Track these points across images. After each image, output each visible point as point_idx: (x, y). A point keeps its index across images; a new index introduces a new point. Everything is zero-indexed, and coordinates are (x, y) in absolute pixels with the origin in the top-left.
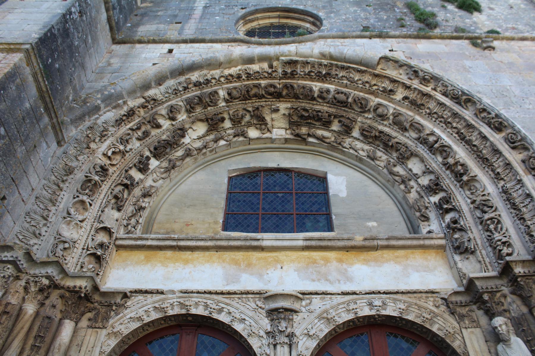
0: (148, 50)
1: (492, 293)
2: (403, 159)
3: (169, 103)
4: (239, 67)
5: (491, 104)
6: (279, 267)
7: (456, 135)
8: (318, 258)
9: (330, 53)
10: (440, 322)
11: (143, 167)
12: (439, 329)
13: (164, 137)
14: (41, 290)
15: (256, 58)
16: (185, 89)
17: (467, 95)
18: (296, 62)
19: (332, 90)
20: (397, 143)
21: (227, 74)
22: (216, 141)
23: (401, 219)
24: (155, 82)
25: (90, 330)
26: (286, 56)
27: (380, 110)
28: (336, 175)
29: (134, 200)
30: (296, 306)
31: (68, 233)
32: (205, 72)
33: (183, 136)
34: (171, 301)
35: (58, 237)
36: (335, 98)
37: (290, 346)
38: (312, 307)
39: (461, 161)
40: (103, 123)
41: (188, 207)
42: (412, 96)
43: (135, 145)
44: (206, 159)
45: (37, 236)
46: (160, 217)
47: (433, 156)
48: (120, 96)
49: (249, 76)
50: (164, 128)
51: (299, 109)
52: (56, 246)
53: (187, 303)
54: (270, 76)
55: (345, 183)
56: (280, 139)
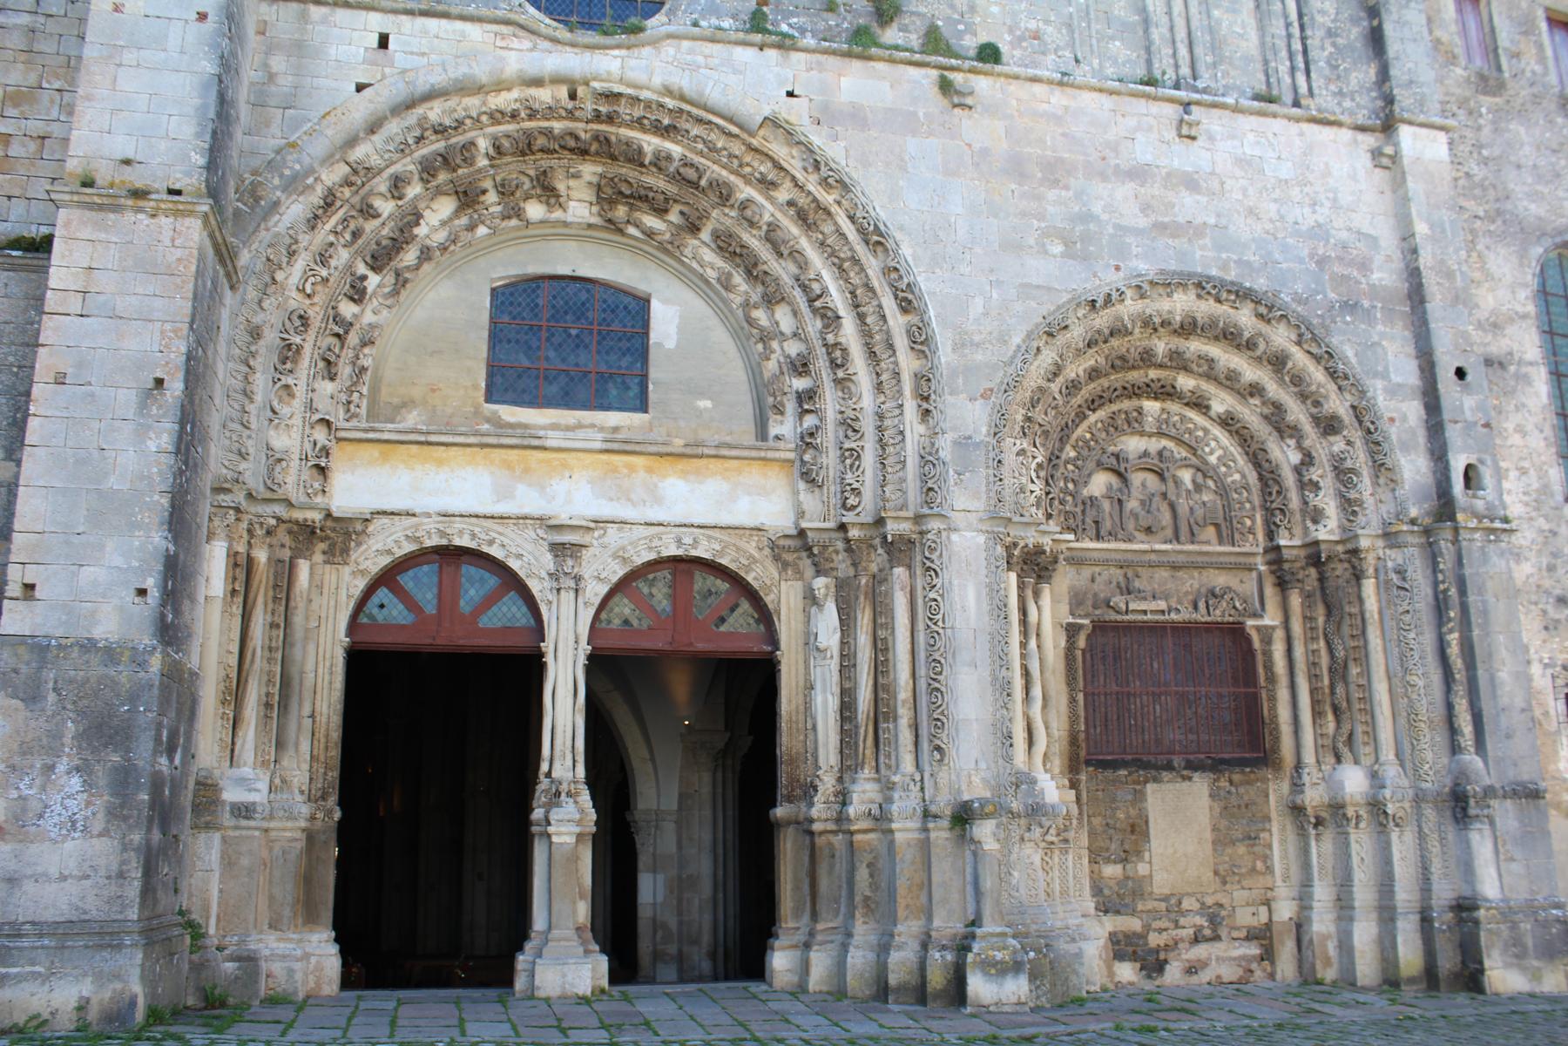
0: (336, 30)
1: (825, 547)
2: (771, 300)
3: (391, 170)
5: (909, 259)
6: (567, 475)
7: (849, 296)
9: (681, 89)
11: (357, 294)
12: (755, 579)
13: (385, 232)
14: (269, 533)
15: (547, 80)
16: (419, 139)
17: (881, 235)
18: (618, 96)
20: (765, 273)
21: (494, 107)
22: (471, 228)
26: (602, 81)
27: (748, 213)
28: (666, 301)
29: (351, 354)
31: (280, 441)
33: (418, 224)
36: (680, 174)
37: (577, 591)
38: (605, 540)
39: (843, 340)
40: (288, 228)
42: (803, 201)
43: (342, 256)
45: (243, 455)
46: (389, 374)
47: (811, 315)
48: (310, 171)
49: (533, 114)
50: (385, 215)
52: (271, 470)
53: (449, 531)
54: (571, 115)
55: (676, 321)
56: (579, 224)
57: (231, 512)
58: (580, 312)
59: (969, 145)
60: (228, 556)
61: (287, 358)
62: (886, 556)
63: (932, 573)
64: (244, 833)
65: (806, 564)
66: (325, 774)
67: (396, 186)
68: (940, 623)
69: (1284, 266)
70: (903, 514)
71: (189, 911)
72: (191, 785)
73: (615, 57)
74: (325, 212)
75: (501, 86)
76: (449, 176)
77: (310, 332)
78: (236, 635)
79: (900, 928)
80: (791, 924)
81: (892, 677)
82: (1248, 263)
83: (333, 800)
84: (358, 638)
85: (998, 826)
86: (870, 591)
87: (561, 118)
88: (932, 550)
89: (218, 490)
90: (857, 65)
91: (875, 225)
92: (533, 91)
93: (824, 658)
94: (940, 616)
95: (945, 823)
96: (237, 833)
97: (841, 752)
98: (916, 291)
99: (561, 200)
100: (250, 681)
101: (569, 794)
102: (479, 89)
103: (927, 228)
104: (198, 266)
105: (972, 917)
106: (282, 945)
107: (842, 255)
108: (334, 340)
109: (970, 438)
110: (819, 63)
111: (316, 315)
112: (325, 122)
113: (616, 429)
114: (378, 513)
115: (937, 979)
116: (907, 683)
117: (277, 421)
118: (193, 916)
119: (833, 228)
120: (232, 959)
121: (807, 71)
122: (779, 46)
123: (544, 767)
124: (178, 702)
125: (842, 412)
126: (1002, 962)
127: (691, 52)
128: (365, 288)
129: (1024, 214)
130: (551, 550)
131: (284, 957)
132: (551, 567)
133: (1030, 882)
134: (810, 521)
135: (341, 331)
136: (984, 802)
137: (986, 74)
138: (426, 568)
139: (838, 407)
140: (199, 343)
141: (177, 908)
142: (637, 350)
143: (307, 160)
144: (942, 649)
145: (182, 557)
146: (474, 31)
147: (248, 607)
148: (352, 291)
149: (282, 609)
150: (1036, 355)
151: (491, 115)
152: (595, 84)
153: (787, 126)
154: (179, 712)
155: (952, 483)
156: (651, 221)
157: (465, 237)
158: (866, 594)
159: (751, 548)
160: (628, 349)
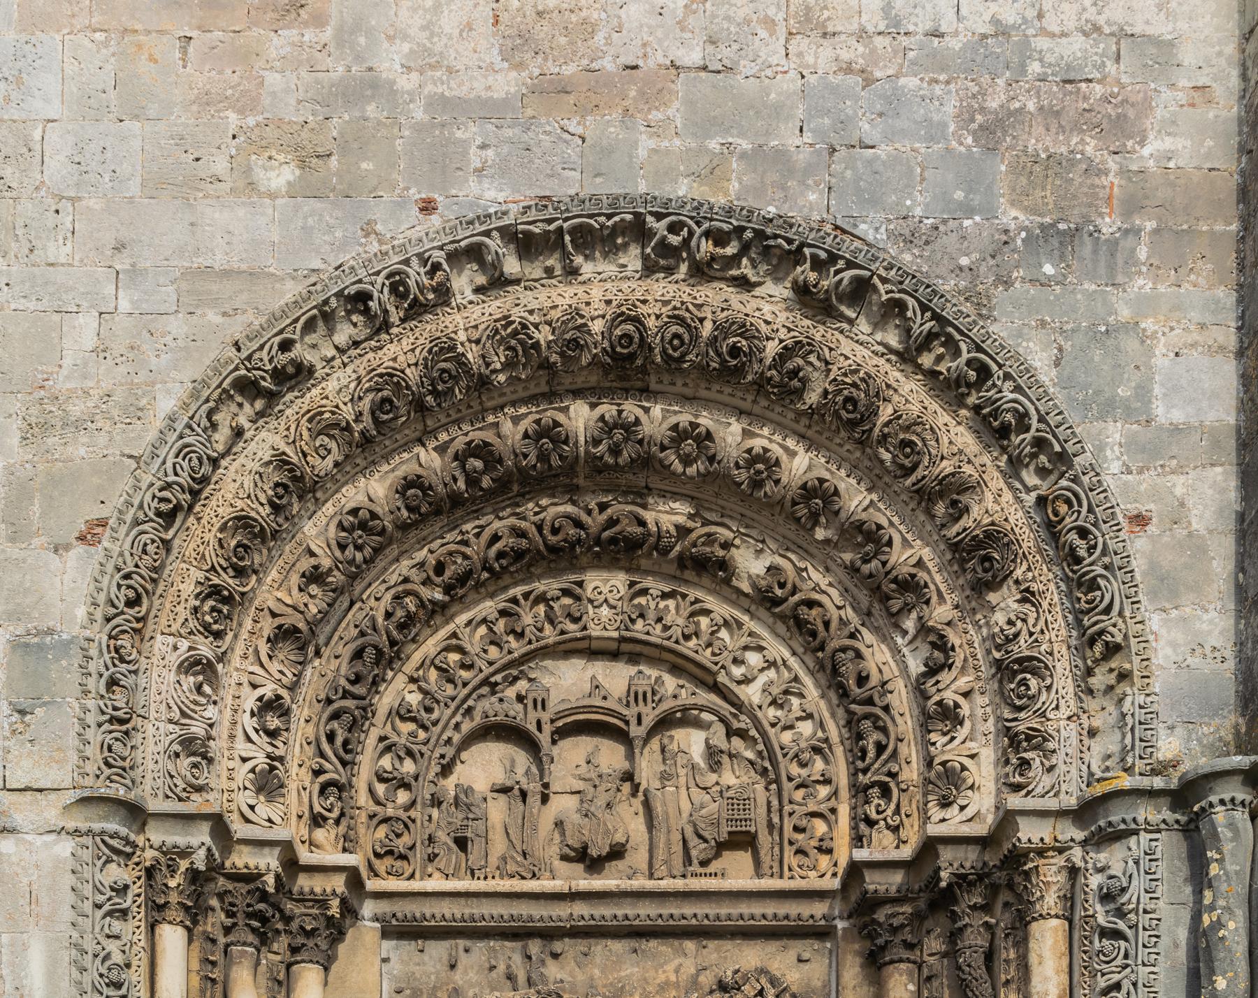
69: (883, 151)
82: (780, 155)
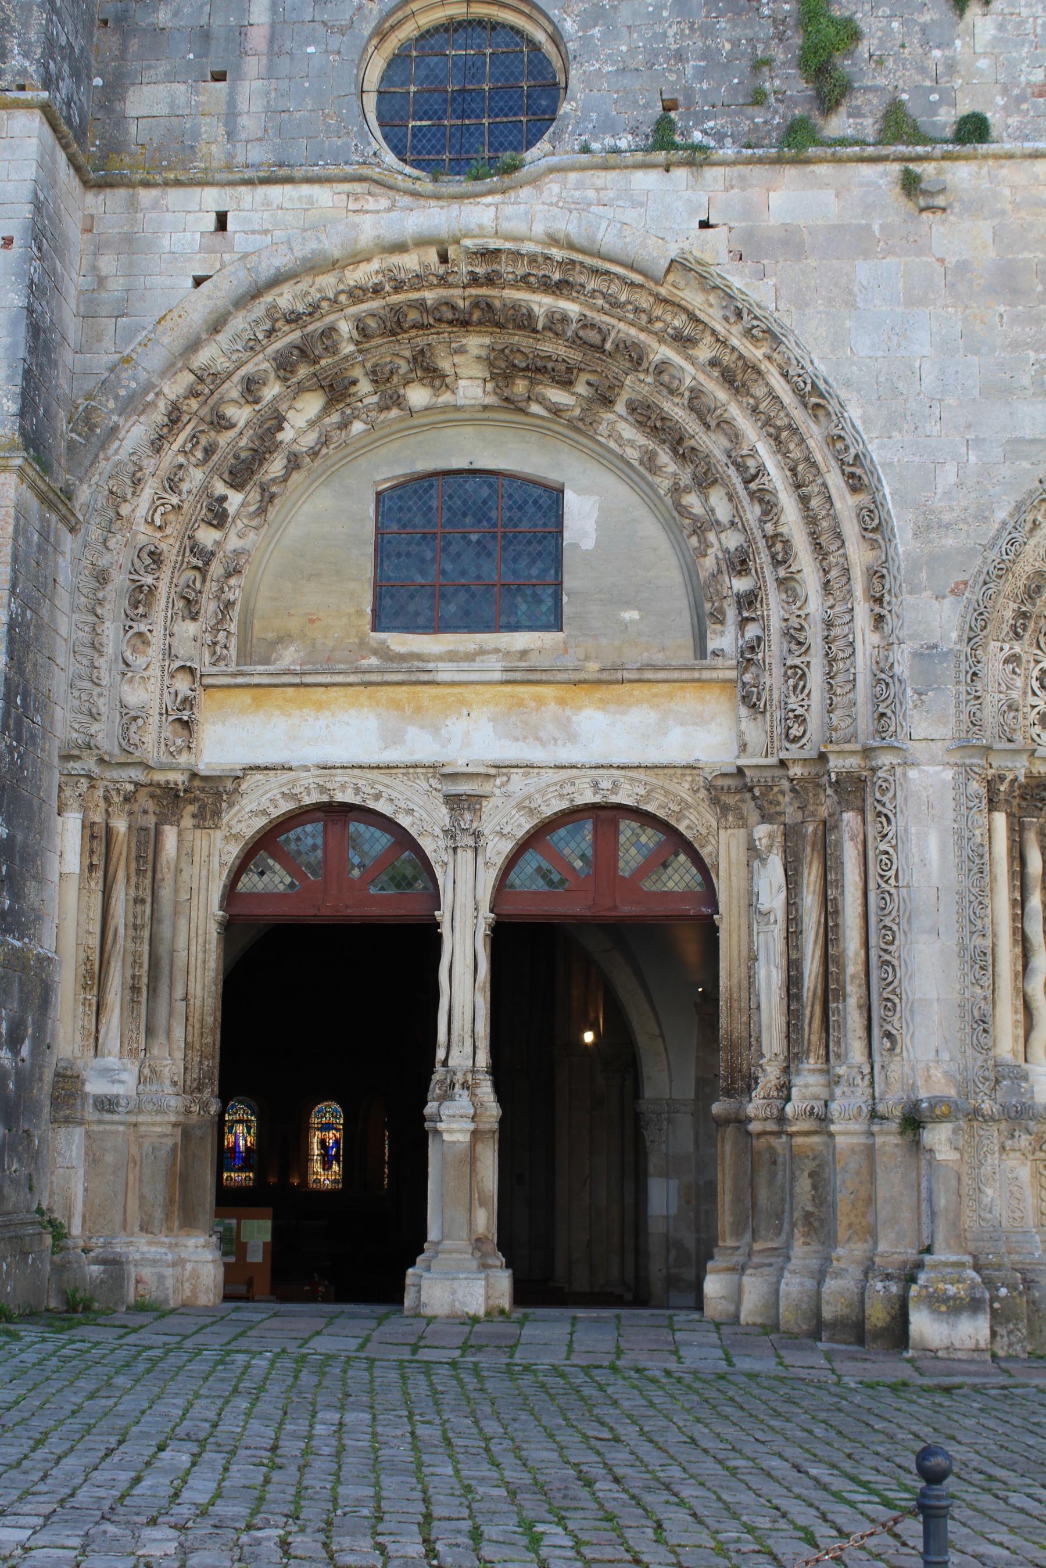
2: (705, 481)
4: (375, 265)
5: (858, 423)
7: (789, 474)
8: (526, 696)
9: (567, 236)
10: (692, 818)
11: (218, 518)
12: (688, 827)
13: (243, 443)
14: (127, 800)
16: (270, 333)
17: (821, 396)
19: (572, 315)
20: (693, 449)
21: (352, 283)
22: (344, 425)
23: (686, 602)
24: (207, 331)
25: (198, 832)
26: (474, 237)
27: (665, 378)
28: (580, 492)
30: (486, 788)
31: (135, 696)
32: (303, 286)
33: (280, 429)
34: (305, 782)
35: (125, 711)
37: (476, 849)
38: (510, 788)
39: (783, 530)
41: (309, 580)
42: (727, 359)
43: (196, 477)
44: (329, 462)
45: (94, 716)
46: (263, 605)
48: (149, 386)
50: (241, 424)
51: (507, 351)
52: (126, 730)
53: (329, 786)
54: (443, 281)
55: (595, 514)
56: (473, 406)
57: (83, 780)
58: (481, 512)
59: (942, 261)
60: (83, 827)
61: (139, 602)
62: (835, 798)
63: (883, 819)
64: (108, 1127)
65: (749, 808)
66: (201, 1063)
67: (249, 390)
68: (892, 881)
70: (847, 747)
71: (50, 1210)
72: (48, 1076)
73: (488, 205)
74: (170, 430)
75: (358, 258)
76: (312, 370)
77: (164, 568)
78: (97, 914)
79: (840, 1251)
80: (730, 1243)
81: (841, 946)
83: (207, 1093)
84: (236, 911)
85: (955, 1131)
86: (819, 840)
87: (432, 286)
88: (884, 791)
89: (67, 758)
90: (791, 172)
91: (813, 384)
92: (396, 259)
93: (768, 923)
94: (892, 872)
95: (894, 1126)
96: (101, 1128)
97: (788, 1037)
98: (867, 463)
99: (447, 380)
100: (113, 964)
101: (465, 1086)
102: (334, 265)
103: (882, 379)
104: (16, 526)
105: (927, 1243)
106: (153, 1249)
107: (779, 423)
108: (191, 574)
109: (935, 646)
110: (742, 178)
111: (170, 548)
112: (160, 328)
113: (524, 654)
114: (251, 768)
115: (877, 1314)
116: (857, 954)
117: (130, 674)
118: (56, 1215)
119: (766, 390)
120: (97, 1261)
121: (726, 190)
122: (689, 163)
123: (441, 1054)
124: (21, 991)
125: (786, 620)
126: (954, 1298)
127: (580, 186)
128: (225, 510)
129: (1016, 345)
130: (446, 803)
131: (154, 1262)
132: (447, 822)
133: (1015, 1203)
134: (753, 756)
135: (200, 564)
136: (935, 1102)
137: (966, 158)
138: (309, 828)
139: (782, 612)
140: (25, 606)
141: (35, 1207)
142: (550, 553)
143: (143, 376)
144: (894, 914)
145: (20, 838)
146: (323, 195)
147: (108, 883)
148: (210, 516)
149: (148, 881)
150: (1031, 531)
151: (350, 294)
152: (467, 242)
153: (699, 268)
154: (24, 1002)
155: (910, 705)
156: (557, 396)
157: (338, 436)
158: (814, 844)
159: (683, 790)
160: (540, 554)
